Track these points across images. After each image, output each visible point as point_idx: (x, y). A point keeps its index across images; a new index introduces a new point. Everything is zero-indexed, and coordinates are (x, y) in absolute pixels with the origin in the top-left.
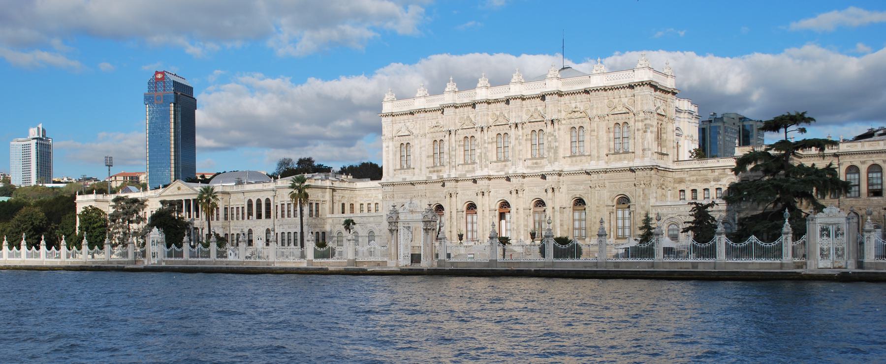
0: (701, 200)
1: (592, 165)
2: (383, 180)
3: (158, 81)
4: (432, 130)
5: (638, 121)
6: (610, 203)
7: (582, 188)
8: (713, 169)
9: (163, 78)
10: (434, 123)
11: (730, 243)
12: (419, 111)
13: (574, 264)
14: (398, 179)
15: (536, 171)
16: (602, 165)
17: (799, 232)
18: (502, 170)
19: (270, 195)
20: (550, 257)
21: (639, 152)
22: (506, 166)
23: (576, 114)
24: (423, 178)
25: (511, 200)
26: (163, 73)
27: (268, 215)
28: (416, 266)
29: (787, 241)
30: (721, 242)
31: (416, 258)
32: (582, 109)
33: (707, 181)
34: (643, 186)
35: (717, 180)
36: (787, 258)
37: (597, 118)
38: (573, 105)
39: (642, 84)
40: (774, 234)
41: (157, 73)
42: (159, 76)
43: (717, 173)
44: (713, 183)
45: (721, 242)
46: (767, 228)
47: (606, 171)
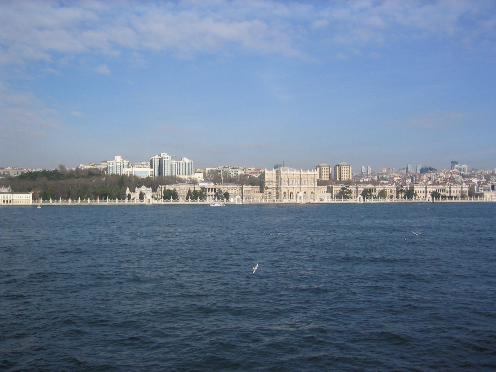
1: (308, 187)
16: (309, 187)
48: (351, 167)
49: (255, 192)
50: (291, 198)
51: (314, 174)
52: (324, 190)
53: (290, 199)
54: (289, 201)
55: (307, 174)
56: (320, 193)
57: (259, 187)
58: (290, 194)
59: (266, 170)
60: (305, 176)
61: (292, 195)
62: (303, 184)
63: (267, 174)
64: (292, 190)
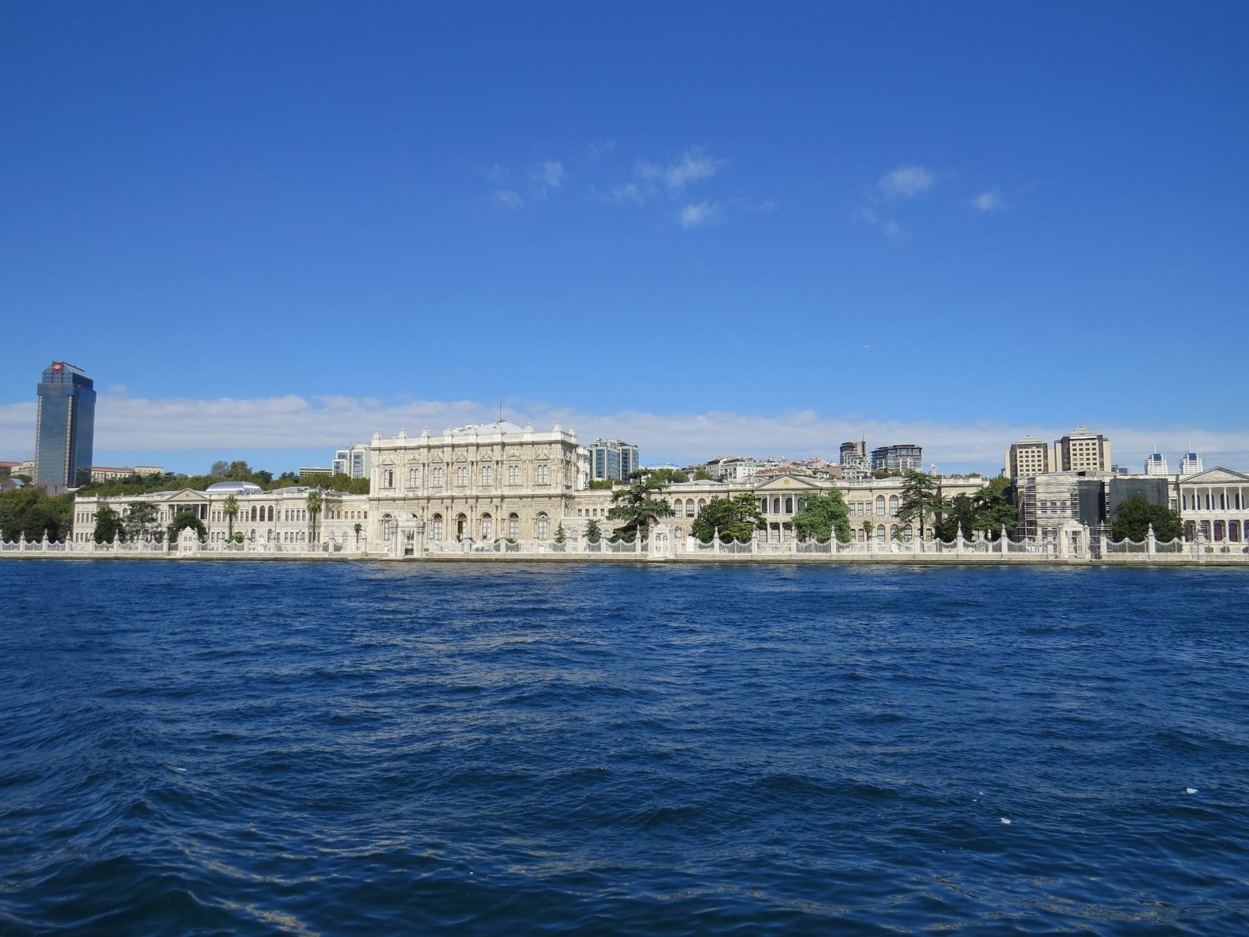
0: (592, 517)
1: (524, 492)
2: (371, 495)
3: (55, 373)
8: (599, 497)
9: (61, 370)
12: (400, 448)
14: (383, 494)
16: (529, 492)
17: (644, 537)
19: (273, 504)
20: (503, 550)
21: (553, 485)
24: (402, 495)
25: (468, 514)
26: (62, 364)
27: (271, 518)
28: (409, 556)
29: (638, 542)
31: (408, 551)
33: (595, 504)
35: (602, 503)
36: (638, 551)
39: (556, 442)
40: (630, 539)
41: (54, 363)
42: (57, 367)
45: (604, 543)
46: (627, 533)
47: (533, 497)
51: (550, 443)
55: (521, 444)
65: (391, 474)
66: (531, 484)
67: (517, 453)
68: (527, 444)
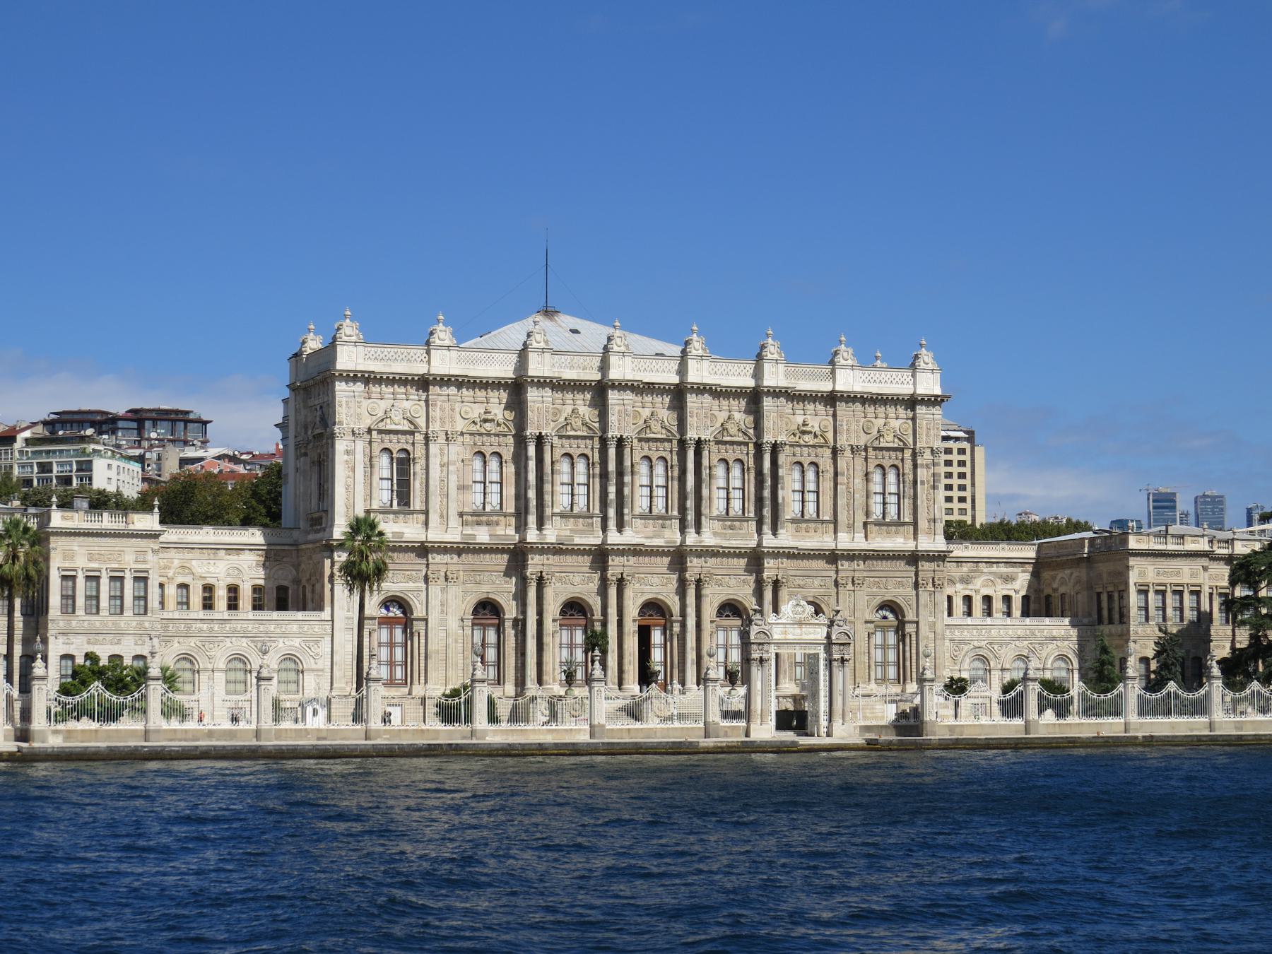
1: (846, 541)
4: (474, 428)
5: (922, 466)
6: (868, 617)
7: (817, 582)
10: (476, 411)
11: (1045, 693)
13: (1172, 725)
15: (734, 543)
16: (858, 542)
18: (658, 537)
22: (663, 526)
23: (806, 438)
24: (454, 534)
30: (1133, 691)
32: (816, 429)
34: (930, 587)
35: (965, 580)
37: (848, 453)
38: (799, 419)
43: (965, 569)
44: (959, 586)
47: (866, 556)
48: (980, 452)
49: (208, 604)
50: (646, 677)
51: (912, 402)
52: (997, 591)
53: (633, 686)
54: (633, 712)
56: (998, 617)
57: (255, 536)
58: (631, 628)
59: (349, 330)
60: (816, 418)
61: (657, 637)
62: (791, 508)
63: (368, 379)
64: (653, 582)
65: (404, 464)
66: (860, 518)
67: (814, 424)
68: (851, 398)
